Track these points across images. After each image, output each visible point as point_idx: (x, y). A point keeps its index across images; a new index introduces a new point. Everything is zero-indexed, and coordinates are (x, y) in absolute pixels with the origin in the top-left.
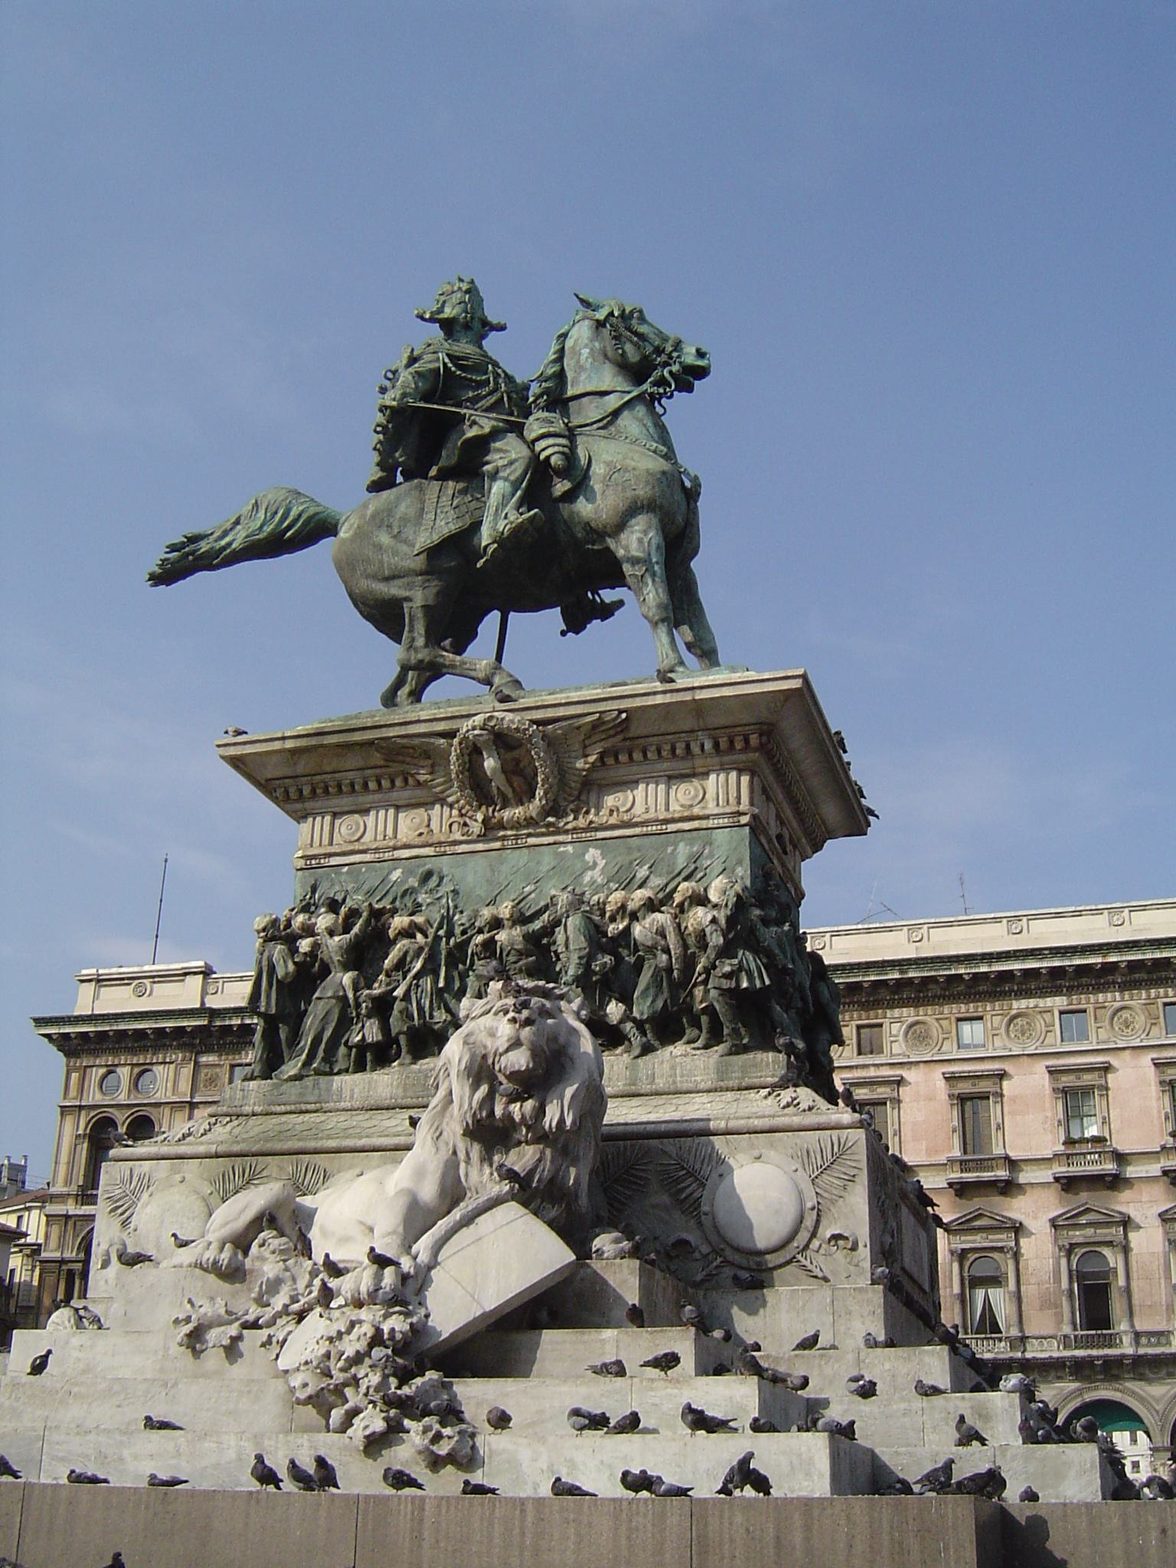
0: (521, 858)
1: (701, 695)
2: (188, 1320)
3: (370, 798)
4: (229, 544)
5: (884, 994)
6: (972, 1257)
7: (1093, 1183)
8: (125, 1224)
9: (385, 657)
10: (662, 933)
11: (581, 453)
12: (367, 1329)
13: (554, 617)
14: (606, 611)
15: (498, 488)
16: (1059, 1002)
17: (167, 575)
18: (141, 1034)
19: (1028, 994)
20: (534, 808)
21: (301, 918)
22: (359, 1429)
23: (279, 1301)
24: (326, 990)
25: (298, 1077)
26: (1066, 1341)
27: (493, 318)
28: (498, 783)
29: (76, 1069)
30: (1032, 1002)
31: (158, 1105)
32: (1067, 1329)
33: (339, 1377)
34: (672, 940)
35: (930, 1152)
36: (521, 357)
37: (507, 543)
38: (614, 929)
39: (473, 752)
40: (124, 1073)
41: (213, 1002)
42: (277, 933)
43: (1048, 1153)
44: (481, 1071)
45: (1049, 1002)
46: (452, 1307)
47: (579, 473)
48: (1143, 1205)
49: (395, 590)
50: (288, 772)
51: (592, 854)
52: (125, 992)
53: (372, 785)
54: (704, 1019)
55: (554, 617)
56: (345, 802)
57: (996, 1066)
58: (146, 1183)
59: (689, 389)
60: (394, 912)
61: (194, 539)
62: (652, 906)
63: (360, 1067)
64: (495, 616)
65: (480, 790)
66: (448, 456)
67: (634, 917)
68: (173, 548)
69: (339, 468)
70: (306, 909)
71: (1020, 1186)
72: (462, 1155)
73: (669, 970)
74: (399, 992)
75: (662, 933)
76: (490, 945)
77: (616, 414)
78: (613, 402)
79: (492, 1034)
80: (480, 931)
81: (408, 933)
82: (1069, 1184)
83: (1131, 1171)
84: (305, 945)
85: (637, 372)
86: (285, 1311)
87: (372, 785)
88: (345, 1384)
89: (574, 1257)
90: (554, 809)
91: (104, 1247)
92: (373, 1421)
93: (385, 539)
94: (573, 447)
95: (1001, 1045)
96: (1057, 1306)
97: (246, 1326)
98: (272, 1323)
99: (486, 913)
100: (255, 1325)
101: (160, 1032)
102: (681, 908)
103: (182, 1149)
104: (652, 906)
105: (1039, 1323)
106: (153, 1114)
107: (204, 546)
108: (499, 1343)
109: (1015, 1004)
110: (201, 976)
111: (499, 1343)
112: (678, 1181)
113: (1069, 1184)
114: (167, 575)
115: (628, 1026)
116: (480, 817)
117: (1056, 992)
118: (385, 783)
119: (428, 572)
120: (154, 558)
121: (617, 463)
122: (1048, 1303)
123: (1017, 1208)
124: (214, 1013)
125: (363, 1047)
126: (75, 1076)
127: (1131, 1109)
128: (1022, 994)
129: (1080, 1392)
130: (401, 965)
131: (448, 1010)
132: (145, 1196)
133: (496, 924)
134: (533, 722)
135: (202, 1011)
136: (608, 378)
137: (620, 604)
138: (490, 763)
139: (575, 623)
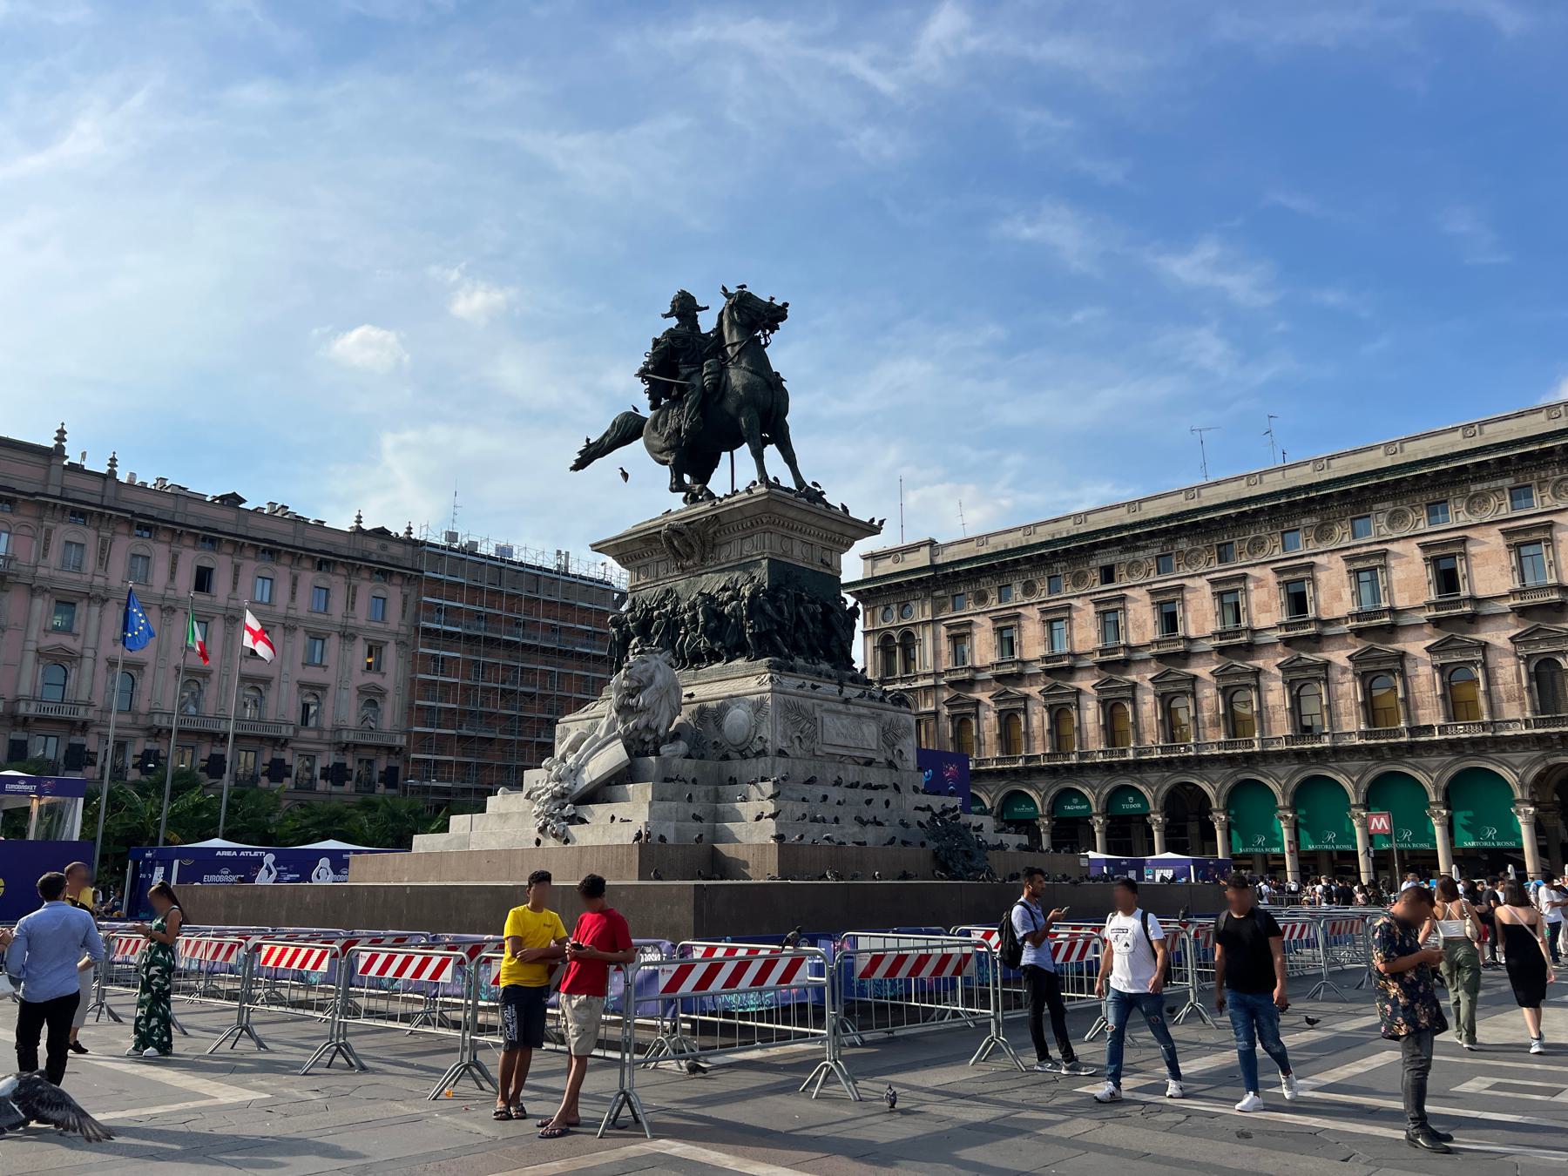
5: (1367, 494)
6: (1449, 670)
16: (1509, 482)
17: (581, 464)
19: (1482, 479)
26: (1362, 735)
27: (700, 303)
30: (1486, 485)
32: (1528, 715)
35: (1411, 599)
39: (669, 539)
40: (894, 607)
41: (939, 560)
43: (1505, 591)
44: (619, 689)
45: (1500, 483)
56: (639, 562)
57: (1460, 533)
65: (677, 554)
67: (726, 604)
90: (703, 559)
95: (1463, 518)
96: (1521, 698)
101: (909, 582)
105: (1511, 711)
106: (912, 629)
109: (1473, 488)
110: (927, 549)
114: (581, 464)
117: (1506, 475)
122: (1215, 724)
123: (1488, 634)
128: (1475, 480)
129: (1544, 758)
135: (933, 567)
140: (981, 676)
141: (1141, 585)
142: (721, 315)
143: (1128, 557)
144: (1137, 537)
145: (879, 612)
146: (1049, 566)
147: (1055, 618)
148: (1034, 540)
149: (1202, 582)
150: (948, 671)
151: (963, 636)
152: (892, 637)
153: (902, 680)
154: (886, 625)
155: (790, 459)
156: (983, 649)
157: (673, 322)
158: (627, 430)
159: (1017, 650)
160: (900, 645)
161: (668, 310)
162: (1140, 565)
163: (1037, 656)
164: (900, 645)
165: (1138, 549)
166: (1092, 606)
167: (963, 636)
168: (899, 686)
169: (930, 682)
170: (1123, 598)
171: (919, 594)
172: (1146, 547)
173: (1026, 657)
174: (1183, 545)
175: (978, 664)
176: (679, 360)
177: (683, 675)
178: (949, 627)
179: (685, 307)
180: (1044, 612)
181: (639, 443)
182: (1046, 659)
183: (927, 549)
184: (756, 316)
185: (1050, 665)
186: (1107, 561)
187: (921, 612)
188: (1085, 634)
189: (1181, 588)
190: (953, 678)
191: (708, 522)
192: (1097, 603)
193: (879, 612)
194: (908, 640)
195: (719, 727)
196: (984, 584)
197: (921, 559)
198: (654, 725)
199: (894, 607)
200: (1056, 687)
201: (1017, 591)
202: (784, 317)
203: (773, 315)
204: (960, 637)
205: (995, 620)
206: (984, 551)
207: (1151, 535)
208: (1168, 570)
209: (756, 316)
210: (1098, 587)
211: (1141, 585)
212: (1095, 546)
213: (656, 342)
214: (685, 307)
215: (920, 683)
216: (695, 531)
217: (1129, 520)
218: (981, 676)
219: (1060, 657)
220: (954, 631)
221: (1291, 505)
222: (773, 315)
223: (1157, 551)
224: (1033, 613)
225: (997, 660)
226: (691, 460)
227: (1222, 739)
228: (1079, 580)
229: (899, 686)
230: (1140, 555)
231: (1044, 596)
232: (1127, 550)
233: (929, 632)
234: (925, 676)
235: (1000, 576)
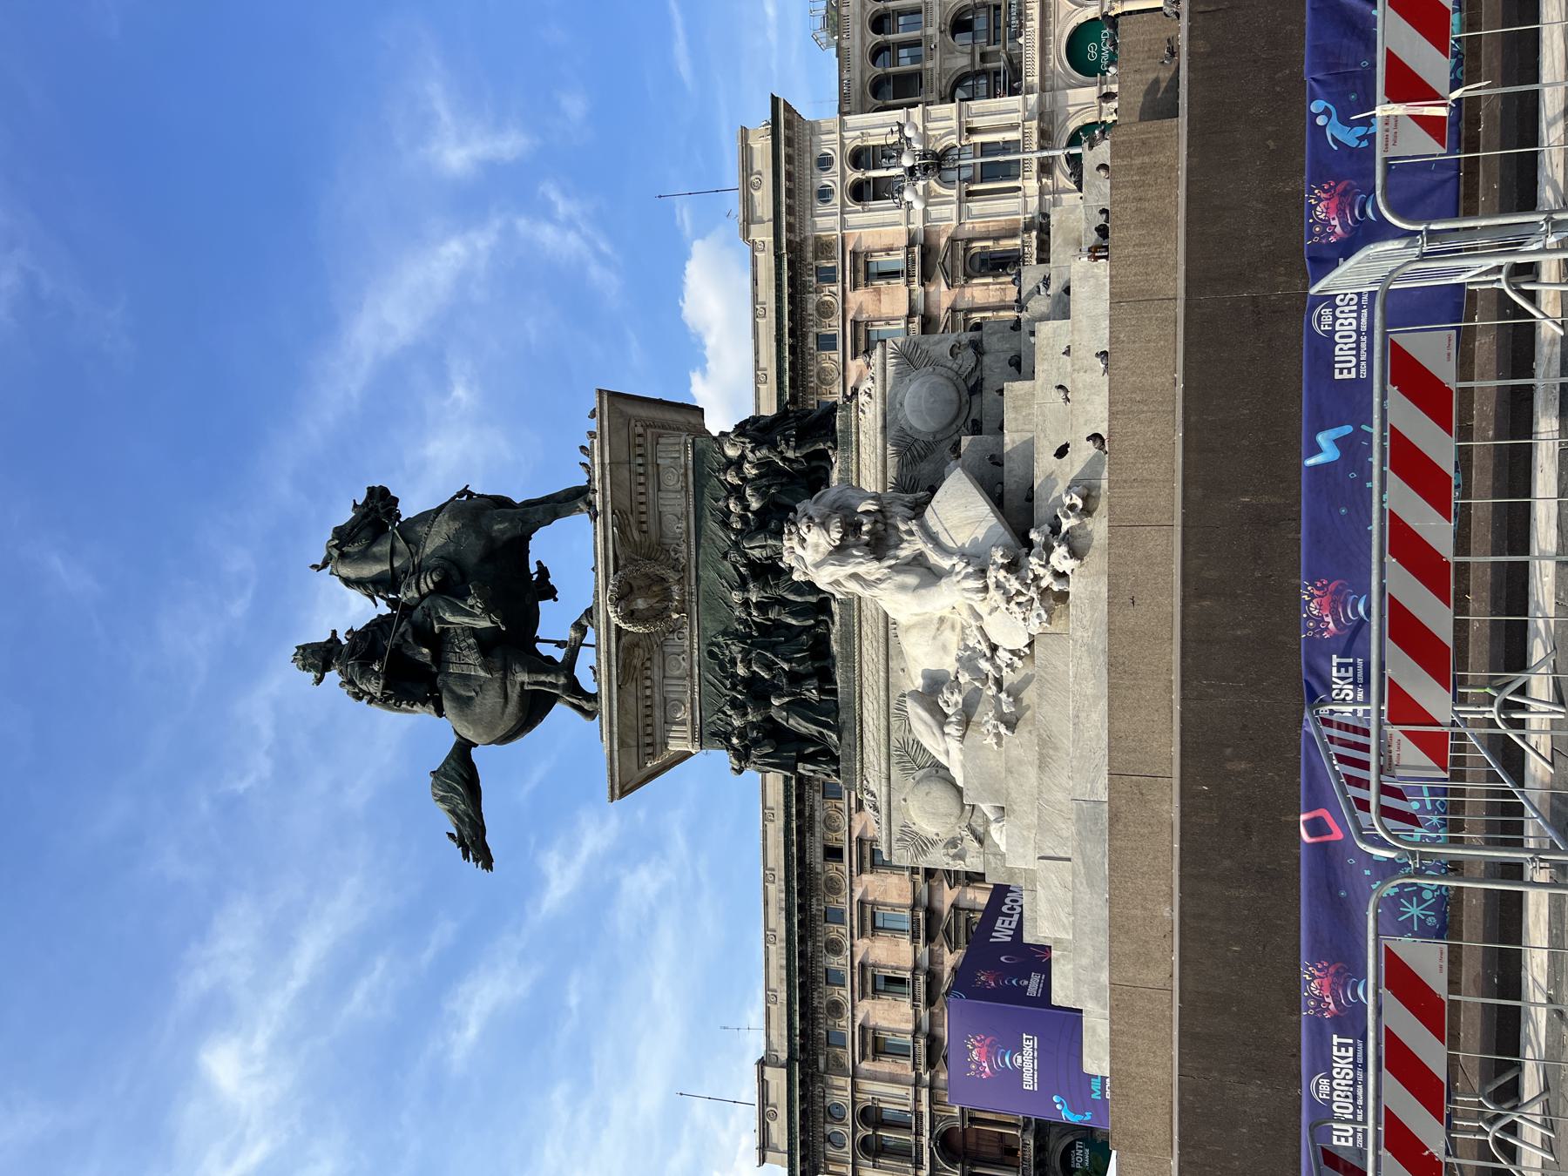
1: (607, 461)
2: (996, 727)
3: (657, 697)
4: (468, 816)
8: (933, 843)
9: (561, 714)
12: (1002, 573)
13: (544, 606)
14: (543, 572)
18: (803, 1113)
20: (672, 576)
21: (735, 741)
22: (1067, 565)
23: (985, 665)
24: (780, 716)
25: (840, 739)
29: (826, 1167)
31: (854, 1103)
33: (1033, 593)
40: (829, 1129)
41: (784, 1056)
42: (742, 756)
44: (840, 552)
47: (446, 564)
49: (514, 694)
50: (634, 750)
52: (773, 1126)
53: (648, 692)
54: (814, 464)
55: (544, 606)
56: (658, 713)
60: (734, 675)
62: (741, 499)
63: (834, 692)
64: (538, 645)
68: (466, 856)
69: (422, 734)
70: (727, 738)
72: (893, 562)
73: (782, 485)
74: (786, 667)
76: (759, 606)
79: (817, 546)
80: (750, 614)
81: (748, 667)
82: (926, 277)
83: (921, 306)
86: (991, 659)
87: (648, 692)
88: (1038, 587)
91: (946, 859)
92: (1060, 558)
97: (1000, 689)
98: (999, 669)
99: (739, 612)
100: (999, 682)
102: (744, 479)
103: (884, 811)
106: (859, 1107)
110: (767, 1069)
112: (913, 457)
116: (675, 616)
118: (648, 683)
119: (506, 670)
120: (472, 868)
124: (791, 1058)
125: (821, 691)
126: (831, 1168)
130: (769, 666)
131: (800, 634)
132: (914, 828)
133: (746, 603)
134: (615, 572)
136: (383, 548)
137: (539, 563)
139: (550, 593)
140: (925, 1026)
141: (850, 819)
142: (348, 582)
143: (819, 828)
144: (800, 813)
145: (831, 1152)
146: (813, 918)
147: (871, 921)
148: (782, 933)
150: (915, 1067)
151: (876, 1039)
152: (865, 1138)
153: (918, 1133)
154: (849, 1143)
156: (894, 1016)
157: (333, 677)
159: (900, 974)
160: (876, 1129)
161: (312, 675)
162: (829, 816)
163: (910, 949)
164: (876, 1129)
165: (812, 816)
166: (865, 877)
167: (876, 1039)
168: (925, 1140)
169: (925, 1093)
170: (861, 841)
171: (818, 1091)
172: (812, 807)
173: (910, 964)
175: (910, 1027)
176: (391, 664)
178: (863, 1057)
180: (862, 934)
182: (915, 937)
183: (767, 1069)
185: (922, 934)
186: (819, 852)
187: (840, 1092)
190: (923, 1060)
191: (622, 527)
192: (861, 871)
193: (831, 1152)
194: (870, 1116)
196: (821, 1002)
197: (777, 1078)
199: (829, 1129)
200: (947, 932)
201: (837, 962)
204: (877, 1045)
205: (863, 995)
206: (783, 996)
207: (800, 798)
210: (845, 866)
211: (850, 819)
212: (801, 860)
215: (925, 1109)
216: (631, 561)
217: (781, 822)
218: (925, 1026)
219: (915, 921)
220: (869, 1050)
223: (818, 797)
224: (862, 945)
225: (909, 1000)
228: (833, 887)
229: (925, 1140)
230: (819, 815)
231: (845, 930)
232: (811, 828)
233: (866, 1085)
234: (917, 1100)
235: (814, 980)
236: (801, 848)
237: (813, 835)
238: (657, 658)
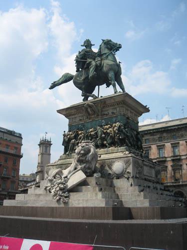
0: (94, 122)
7: (176, 160)
10: (111, 131)
11: (102, 63)
15: (91, 69)
17: (52, 88)
20: (95, 116)
27: (92, 43)
28: (90, 112)
34: (112, 132)
36: (95, 49)
37: (93, 77)
38: (105, 131)
46: (71, 183)
48: (184, 163)
51: (103, 121)
56: (73, 116)
58: (50, 169)
59: (119, 50)
61: (55, 82)
62: (110, 128)
64: (97, 87)
66: (85, 66)
67: (108, 129)
68: (52, 84)
71: (167, 161)
75: (111, 131)
77: (108, 56)
78: (107, 54)
84: (68, 137)
85: (110, 49)
89: (86, 177)
93: (78, 79)
94: (101, 62)
104: (110, 128)
107: (56, 83)
108: (76, 188)
111: (76, 188)
113: (173, 160)
114: (52, 88)
115: (107, 144)
121: (107, 62)
127: (182, 150)
130: (80, 138)
138: (89, 110)
143: (152, 137)
144: (154, 132)
149: (169, 144)
155: (122, 88)
157: (84, 48)
158: (67, 79)
161: (83, 44)
165: (154, 135)
172: (156, 135)
174: (165, 135)
177: (100, 151)
179: (88, 44)
181: (72, 82)
184: (111, 47)
188: (168, 152)
189: (164, 145)
195: (110, 168)
198: (91, 166)
202: (120, 47)
203: (117, 47)
207: (157, 132)
208: (162, 141)
209: (111, 47)
213: (80, 53)
214: (88, 44)
221: (179, 128)
222: (117, 47)
223: (159, 136)
226: (87, 87)
227: (173, 181)
230: (155, 137)
236: (146, 134)
237: (151, 136)
238: (82, 115)
